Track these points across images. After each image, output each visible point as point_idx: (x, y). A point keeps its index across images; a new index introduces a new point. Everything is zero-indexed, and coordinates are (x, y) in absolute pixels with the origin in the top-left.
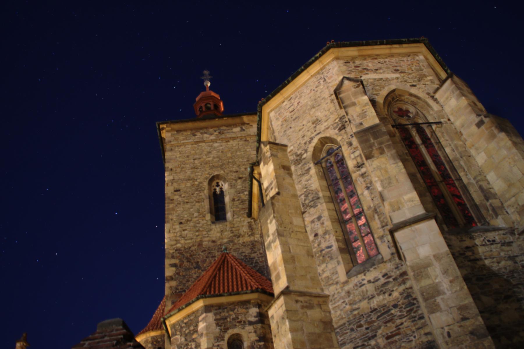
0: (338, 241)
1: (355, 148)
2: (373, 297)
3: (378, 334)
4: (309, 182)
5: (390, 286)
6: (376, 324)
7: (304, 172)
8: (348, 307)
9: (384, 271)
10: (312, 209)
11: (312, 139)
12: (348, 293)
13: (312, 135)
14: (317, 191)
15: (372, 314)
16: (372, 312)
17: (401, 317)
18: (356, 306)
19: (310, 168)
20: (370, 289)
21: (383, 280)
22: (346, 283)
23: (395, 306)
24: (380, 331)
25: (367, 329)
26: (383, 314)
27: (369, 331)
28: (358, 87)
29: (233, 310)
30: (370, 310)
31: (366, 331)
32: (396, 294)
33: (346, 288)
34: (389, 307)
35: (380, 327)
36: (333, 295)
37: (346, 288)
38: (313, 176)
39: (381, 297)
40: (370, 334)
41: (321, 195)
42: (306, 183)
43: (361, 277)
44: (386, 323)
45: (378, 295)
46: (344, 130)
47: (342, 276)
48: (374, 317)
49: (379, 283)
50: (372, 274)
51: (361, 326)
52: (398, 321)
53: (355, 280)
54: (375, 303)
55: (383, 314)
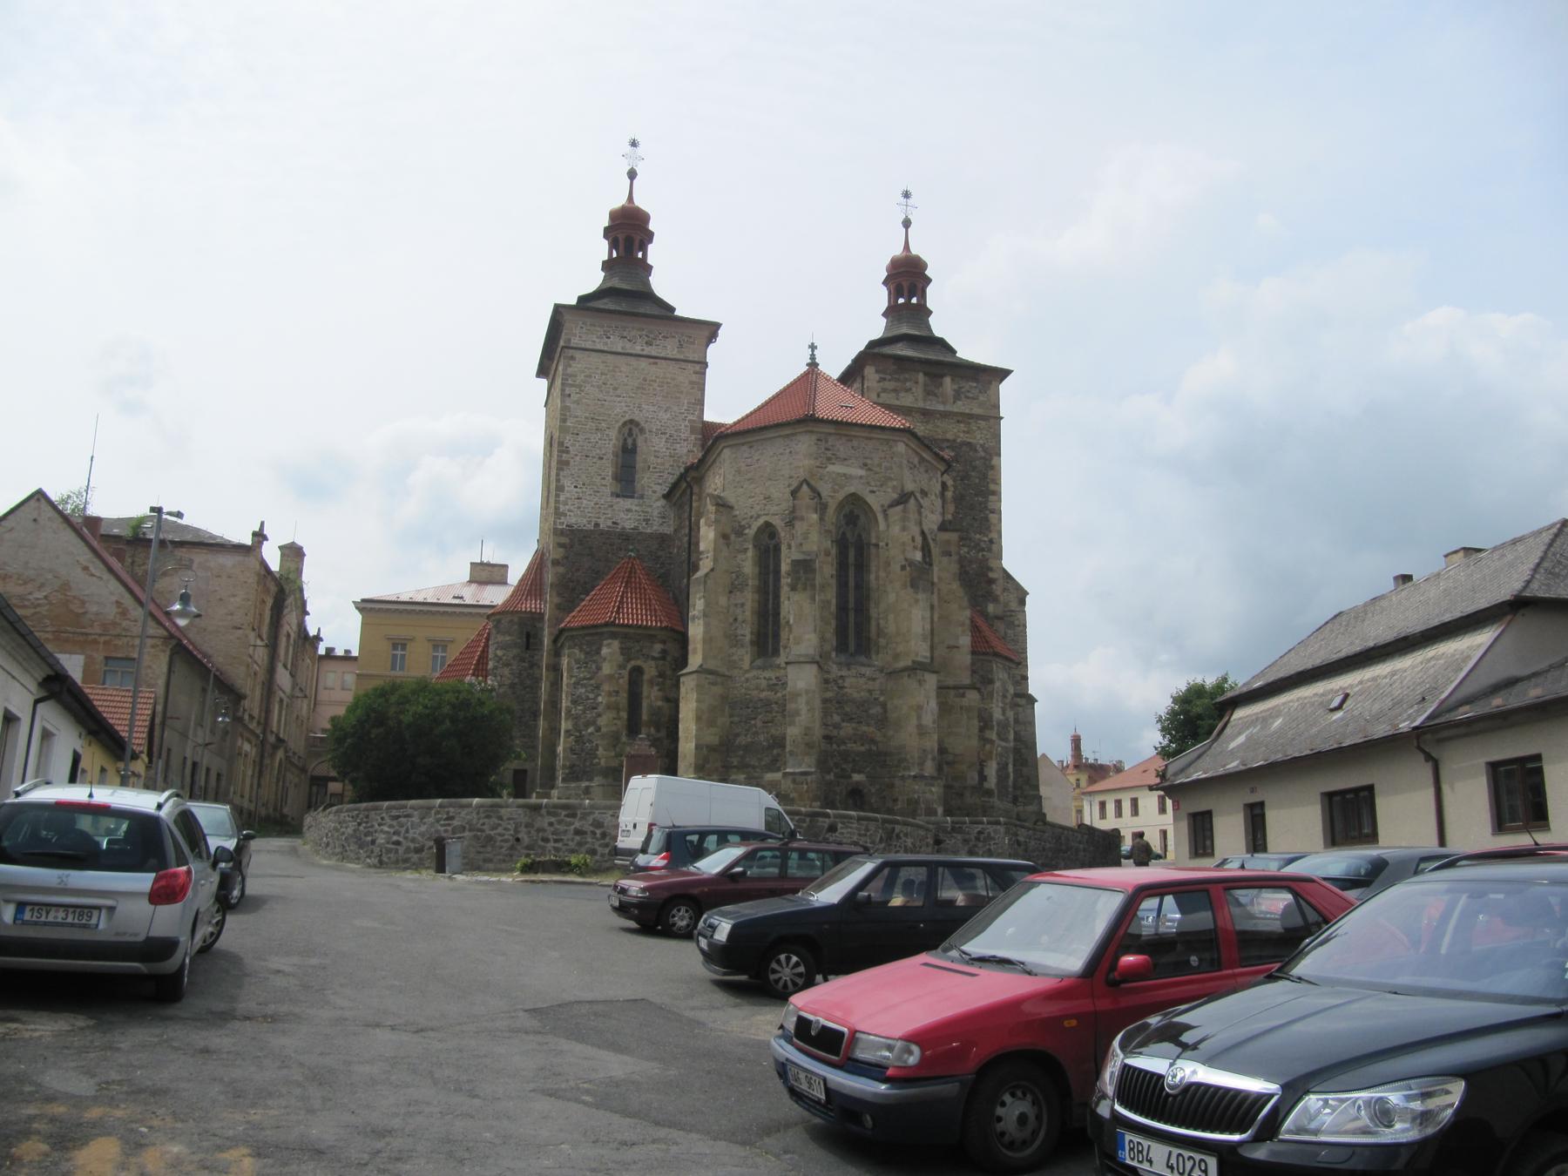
0: (752, 633)
2: (763, 690)
5: (777, 687)
8: (743, 690)
9: (778, 674)
12: (747, 680)
17: (777, 712)
18: (749, 692)
20: (764, 683)
21: (774, 681)
22: (747, 671)
23: (776, 703)
28: (812, 499)
29: (638, 642)
32: (779, 695)
33: (747, 676)
35: (760, 714)
37: (747, 676)
39: (769, 693)
40: (753, 716)
43: (760, 672)
44: (766, 712)
45: (768, 691)
47: (746, 665)
49: (771, 682)
50: (768, 674)
51: (748, 708)
52: (774, 714)
53: (754, 673)
54: (763, 695)
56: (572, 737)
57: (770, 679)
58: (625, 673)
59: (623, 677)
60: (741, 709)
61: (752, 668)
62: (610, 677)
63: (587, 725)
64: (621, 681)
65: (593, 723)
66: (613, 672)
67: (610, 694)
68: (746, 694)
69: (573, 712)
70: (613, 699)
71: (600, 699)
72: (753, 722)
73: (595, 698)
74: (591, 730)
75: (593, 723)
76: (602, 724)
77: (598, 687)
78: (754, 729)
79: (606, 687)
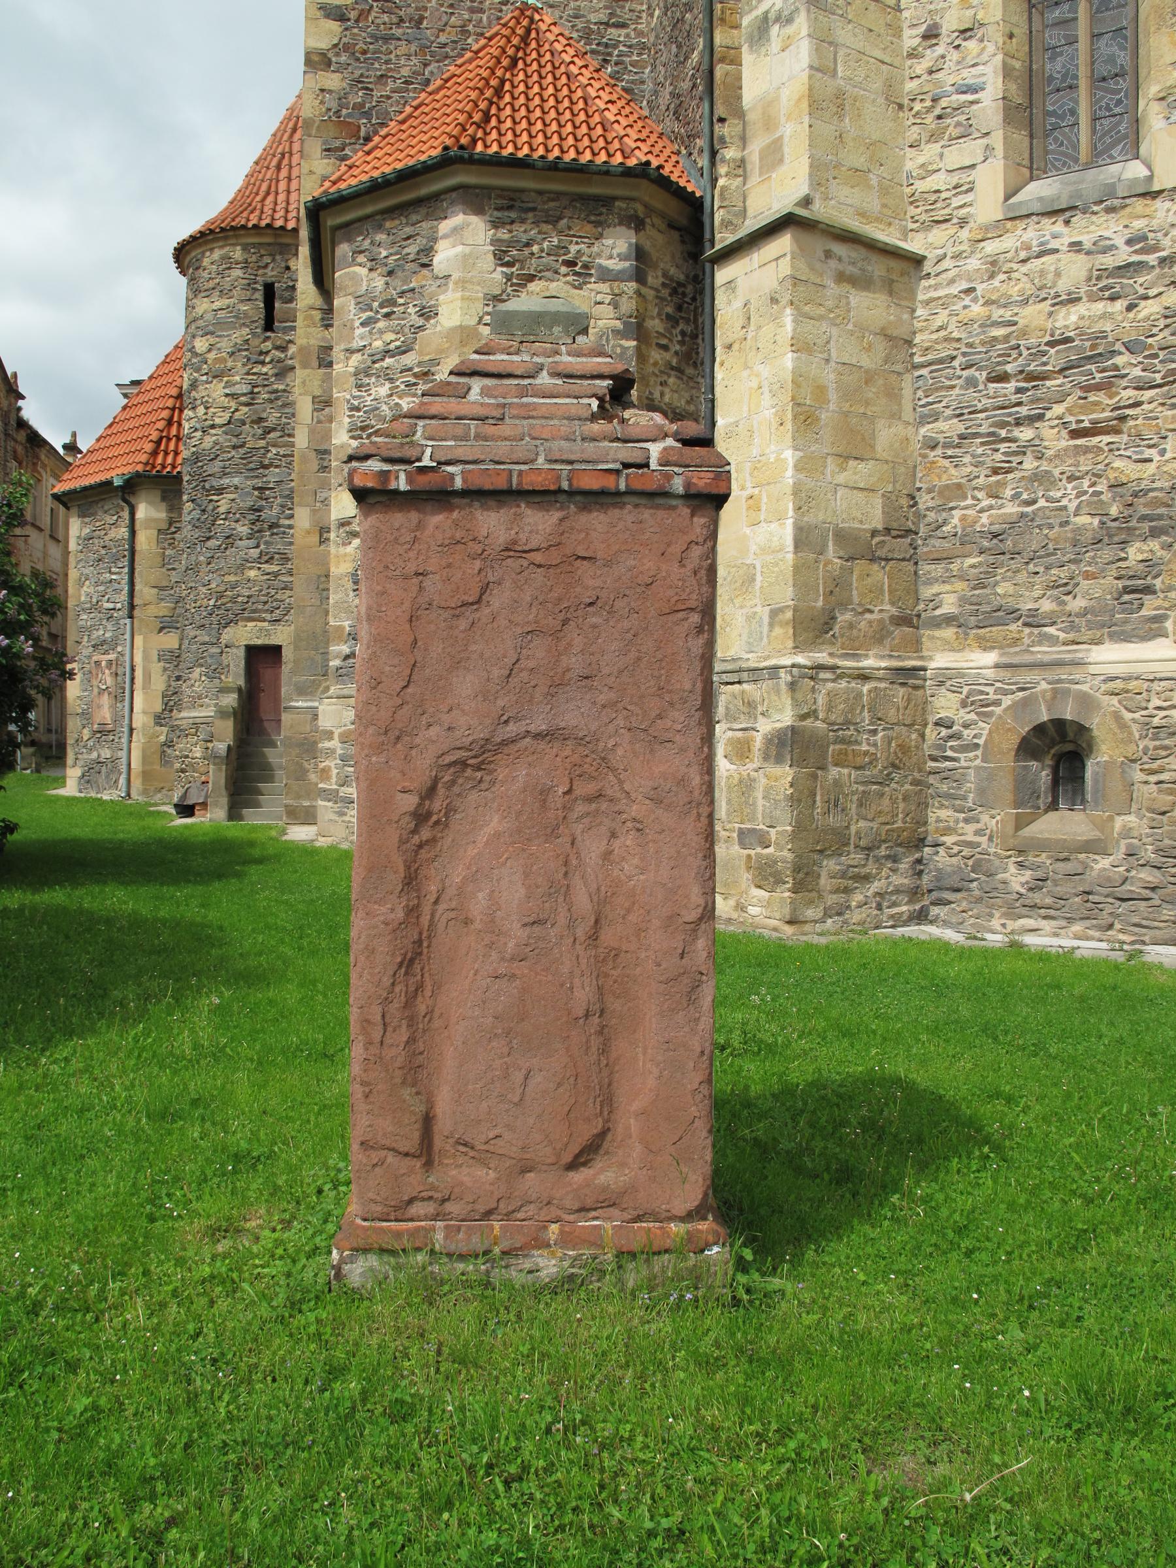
6: (1048, 383)
25: (1019, 391)
27: (1024, 398)
31: (1014, 398)
40: (1024, 411)
44: (1088, 389)
51: (1003, 378)
60: (971, 383)
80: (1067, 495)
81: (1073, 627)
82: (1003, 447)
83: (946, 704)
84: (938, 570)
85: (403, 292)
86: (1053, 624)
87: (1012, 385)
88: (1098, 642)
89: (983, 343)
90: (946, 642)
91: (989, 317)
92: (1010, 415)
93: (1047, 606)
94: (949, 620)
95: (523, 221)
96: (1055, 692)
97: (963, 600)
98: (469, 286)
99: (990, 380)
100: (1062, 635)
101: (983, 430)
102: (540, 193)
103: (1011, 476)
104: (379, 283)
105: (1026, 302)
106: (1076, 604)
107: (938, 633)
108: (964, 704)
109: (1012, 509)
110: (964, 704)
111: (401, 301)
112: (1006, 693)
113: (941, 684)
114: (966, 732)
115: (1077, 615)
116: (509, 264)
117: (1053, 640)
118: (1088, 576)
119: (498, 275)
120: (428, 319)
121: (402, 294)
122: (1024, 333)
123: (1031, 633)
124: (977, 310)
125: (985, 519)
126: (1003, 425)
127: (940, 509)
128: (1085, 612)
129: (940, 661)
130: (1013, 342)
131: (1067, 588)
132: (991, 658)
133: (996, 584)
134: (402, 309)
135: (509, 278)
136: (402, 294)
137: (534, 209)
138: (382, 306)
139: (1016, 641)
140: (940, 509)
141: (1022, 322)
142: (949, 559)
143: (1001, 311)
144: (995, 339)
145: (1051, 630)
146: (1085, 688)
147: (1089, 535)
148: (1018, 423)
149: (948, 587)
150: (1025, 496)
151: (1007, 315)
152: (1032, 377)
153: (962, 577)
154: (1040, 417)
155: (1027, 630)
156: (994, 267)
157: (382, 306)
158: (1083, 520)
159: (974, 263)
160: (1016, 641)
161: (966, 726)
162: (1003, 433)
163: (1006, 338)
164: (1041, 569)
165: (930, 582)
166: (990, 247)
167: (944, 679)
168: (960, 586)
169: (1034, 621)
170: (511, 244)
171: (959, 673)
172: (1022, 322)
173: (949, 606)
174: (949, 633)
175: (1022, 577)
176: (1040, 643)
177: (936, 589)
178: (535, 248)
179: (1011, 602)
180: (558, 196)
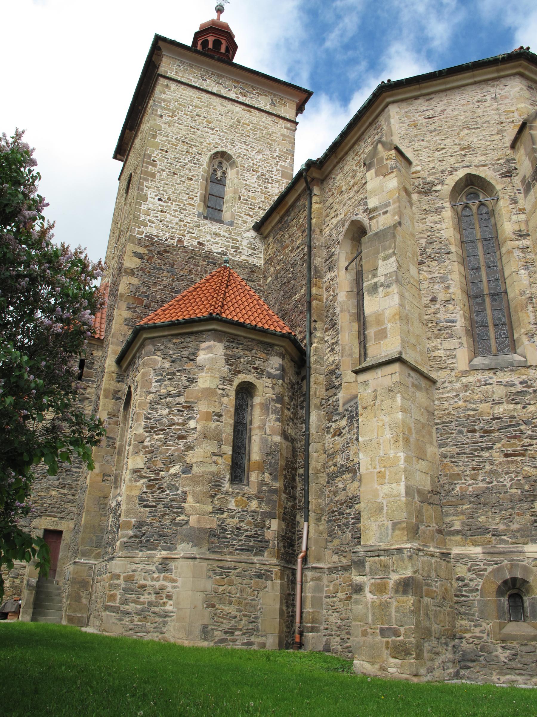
1: (520, 210)
3: (495, 447)
4: (439, 226)
6: (493, 434)
7: (432, 209)
10: (435, 263)
11: (455, 169)
13: (457, 165)
14: (447, 242)
15: (494, 422)
16: (493, 419)
19: (443, 208)
20: (500, 392)
24: (499, 445)
25: (481, 437)
26: (509, 426)
27: (484, 439)
30: (491, 417)
31: (480, 439)
34: (518, 421)
36: (444, 383)
38: (446, 220)
40: (484, 445)
41: (453, 249)
42: (432, 225)
46: (509, 179)
48: (495, 425)
51: (474, 431)
55: (509, 426)
56: (143, 481)
57: (510, 384)
58: (232, 390)
59: (228, 396)
61: (473, 369)
62: (209, 393)
63: (169, 462)
64: (225, 400)
65: (180, 459)
66: (214, 387)
67: (208, 417)
68: (466, 409)
69: (146, 443)
70: (213, 425)
71: (192, 424)
72: (486, 454)
73: (183, 424)
74: (175, 469)
75: (180, 459)
76: (194, 460)
77: (189, 407)
78: (488, 467)
79: (203, 407)
80: (506, 480)
81: (514, 537)
82: (476, 459)
83: (461, 570)
84: (451, 510)
85: (180, 370)
86: (505, 535)
87: (478, 435)
88: (526, 543)
89: (464, 417)
90: (457, 542)
91: (466, 407)
92: (479, 446)
93: (502, 527)
94: (458, 532)
95: (238, 348)
96: (512, 565)
97: (463, 524)
98: (214, 371)
99: (469, 431)
100: (510, 540)
101: (467, 451)
102: (245, 338)
103: (480, 471)
104: (167, 365)
105: (481, 402)
106: (515, 526)
107: (453, 538)
108: (469, 570)
109: (482, 485)
110: (469, 570)
111: (179, 374)
112: (489, 565)
113: (458, 561)
114: (471, 583)
115: (515, 531)
116: (230, 365)
117: (506, 542)
118: (518, 514)
119: (226, 368)
120: (192, 383)
121: (179, 371)
122: (481, 414)
123: (496, 539)
124: (461, 403)
125: (470, 489)
126: (476, 450)
127: (450, 484)
128: (518, 531)
129: (455, 551)
130: (477, 417)
131: (509, 520)
132: (479, 550)
133: (478, 517)
134: (178, 377)
135: (230, 370)
136: (179, 371)
137: (242, 344)
138: (168, 375)
139: (489, 542)
140: (450, 484)
141: (480, 410)
142: (456, 505)
143: (471, 405)
144: (469, 415)
145: (505, 538)
146: (525, 563)
147: (517, 497)
148: (482, 449)
149: (456, 518)
150: (488, 480)
151: (474, 406)
152: (486, 431)
153: (462, 513)
154: (491, 448)
155: (494, 538)
156: (466, 387)
157: (168, 375)
158: (514, 491)
159: (458, 385)
160: (489, 542)
161: (471, 580)
162: (476, 453)
163: (474, 416)
164: (498, 511)
165: (448, 515)
166: (465, 380)
167: (459, 558)
168: (462, 517)
169: (496, 533)
170: (232, 356)
171: (467, 556)
172: (480, 410)
173: (457, 526)
174: (458, 538)
175: (489, 514)
176: (500, 543)
177: (450, 518)
178: (242, 360)
179: (486, 525)
180: (253, 340)
